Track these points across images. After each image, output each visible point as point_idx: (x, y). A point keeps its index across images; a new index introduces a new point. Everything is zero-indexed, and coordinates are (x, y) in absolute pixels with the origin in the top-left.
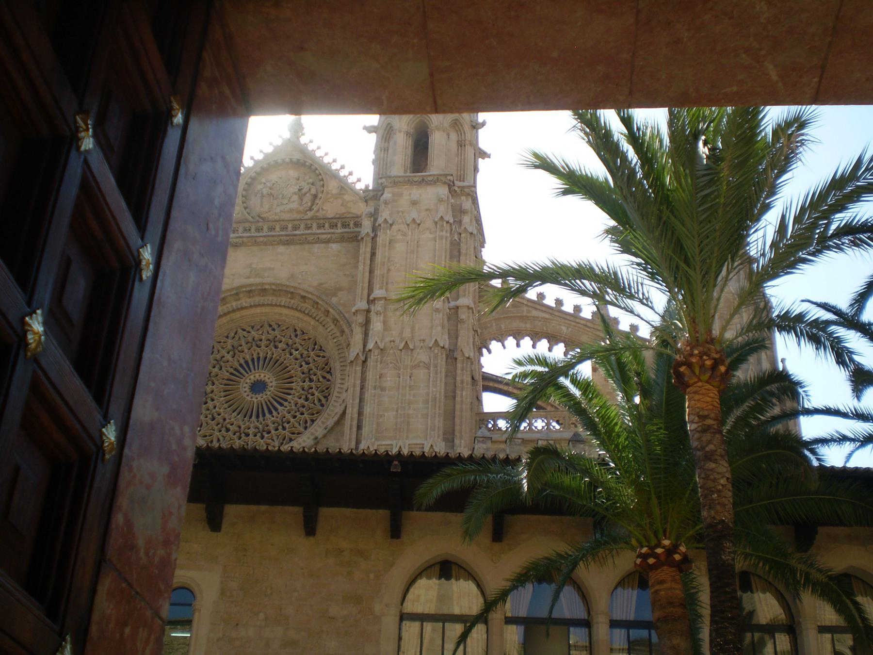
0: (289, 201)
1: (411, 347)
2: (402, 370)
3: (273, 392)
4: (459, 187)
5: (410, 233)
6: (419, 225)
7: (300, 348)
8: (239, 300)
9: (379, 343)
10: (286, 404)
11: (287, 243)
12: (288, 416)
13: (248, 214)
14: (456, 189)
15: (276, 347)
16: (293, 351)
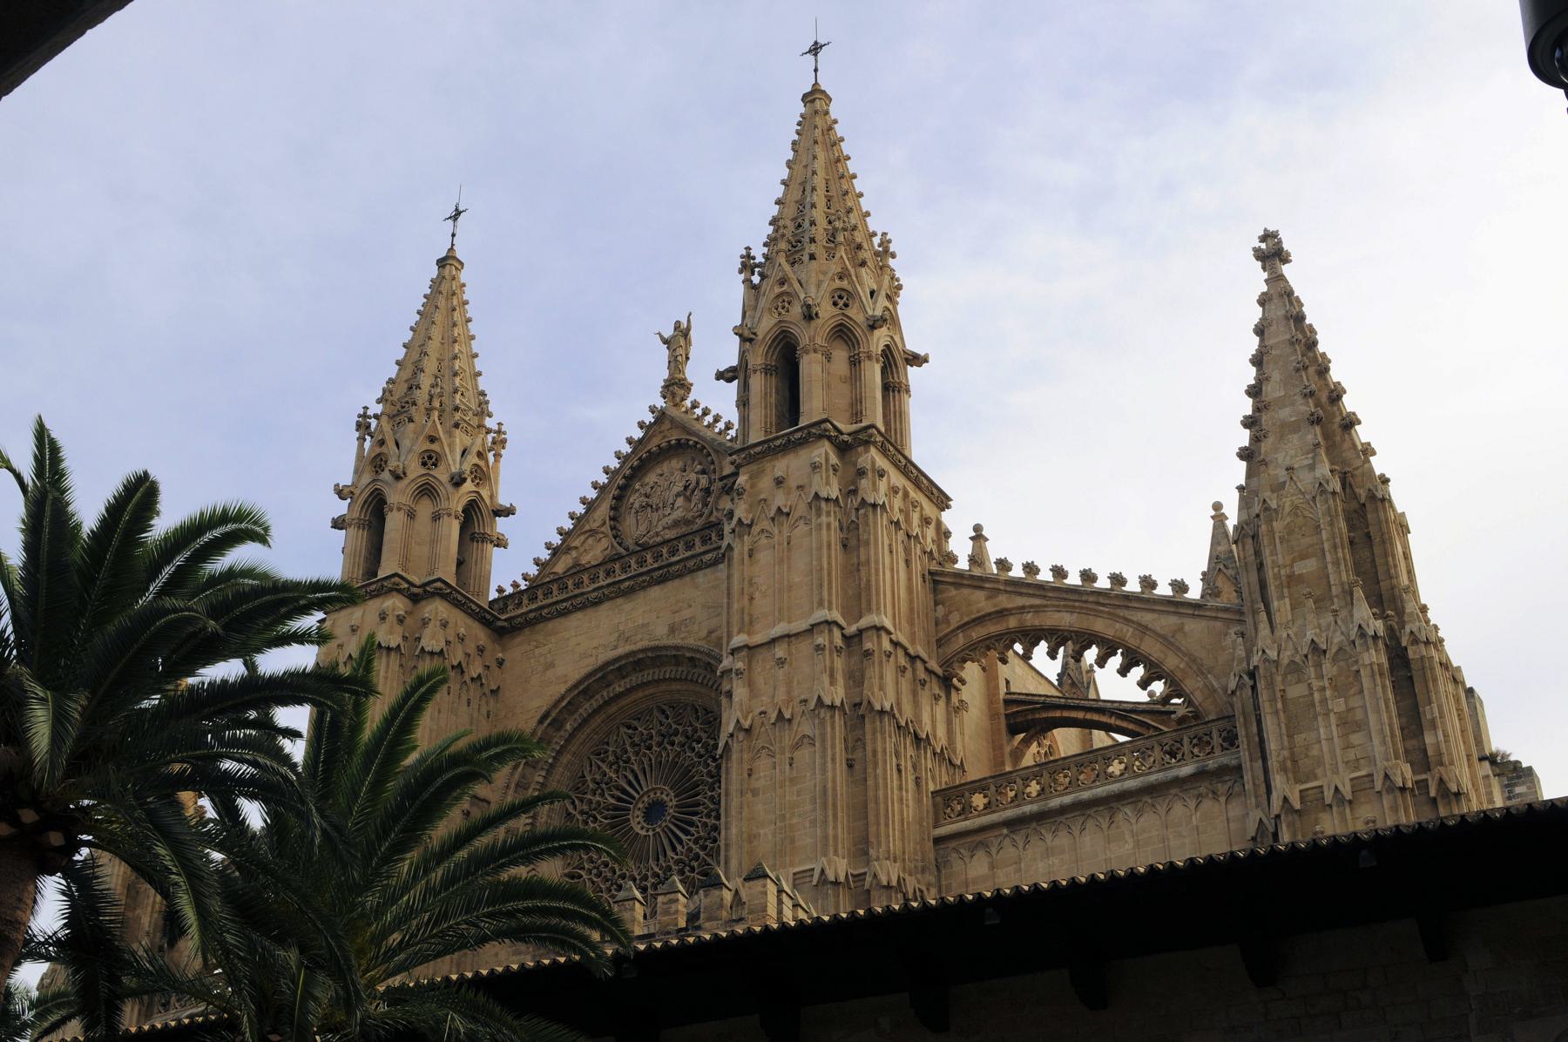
0: (672, 509)
1: (787, 716)
2: (777, 756)
3: (673, 816)
4: (849, 434)
5: (776, 532)
6: (788, 514)
7: (704, 736)
8: (608, 686)
9: (742, 721)
10: (692, 830)
11: (662, 580)
12: (696, 849)
13: (620, 544)
14: (846, 438)
15: (649, 748)
16: (694, 744)
